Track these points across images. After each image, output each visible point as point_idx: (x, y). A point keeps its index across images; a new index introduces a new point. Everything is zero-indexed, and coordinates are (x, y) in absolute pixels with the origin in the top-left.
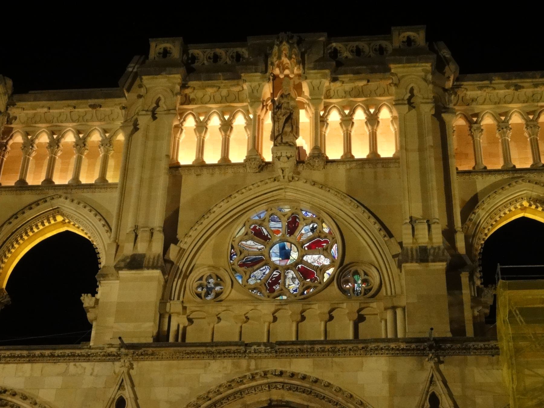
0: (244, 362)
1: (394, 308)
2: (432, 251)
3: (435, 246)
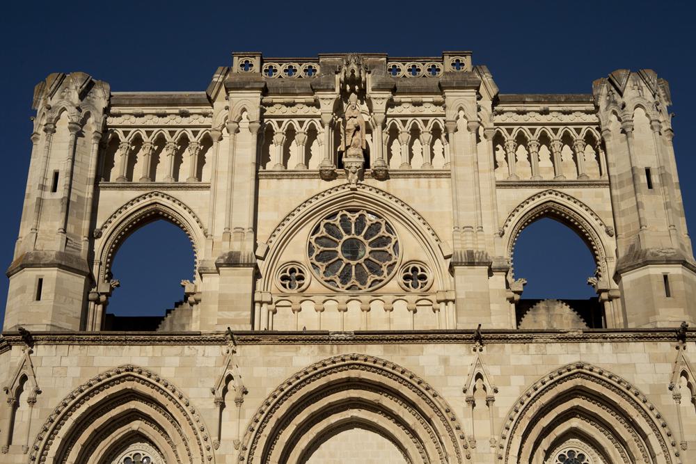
0: (328, 347)
1: (446, 302)
2: (477, 255)
3: (480, 250)
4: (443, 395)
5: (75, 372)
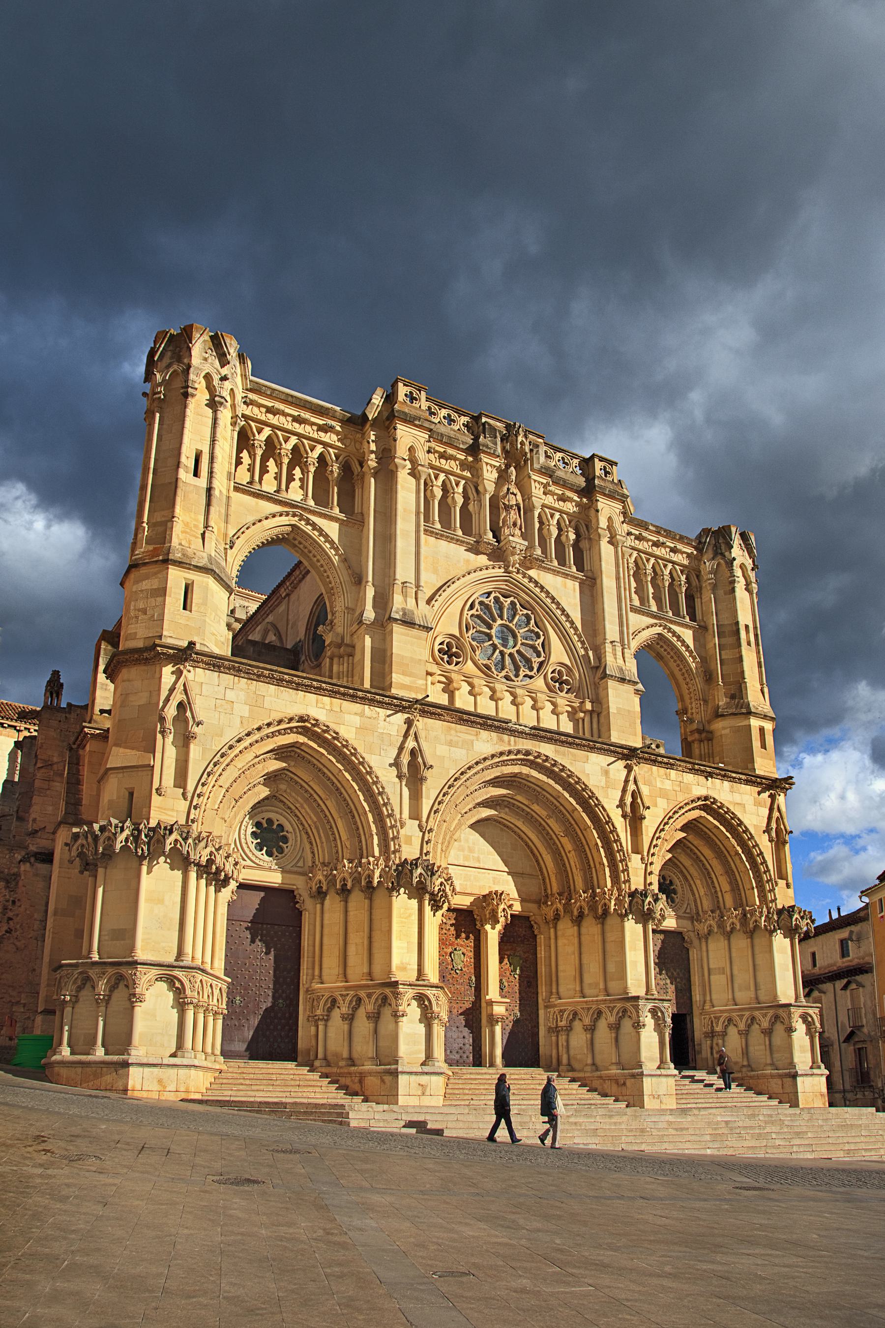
0: (506, 737)
4: (606, 806)
5: (243, 710)
